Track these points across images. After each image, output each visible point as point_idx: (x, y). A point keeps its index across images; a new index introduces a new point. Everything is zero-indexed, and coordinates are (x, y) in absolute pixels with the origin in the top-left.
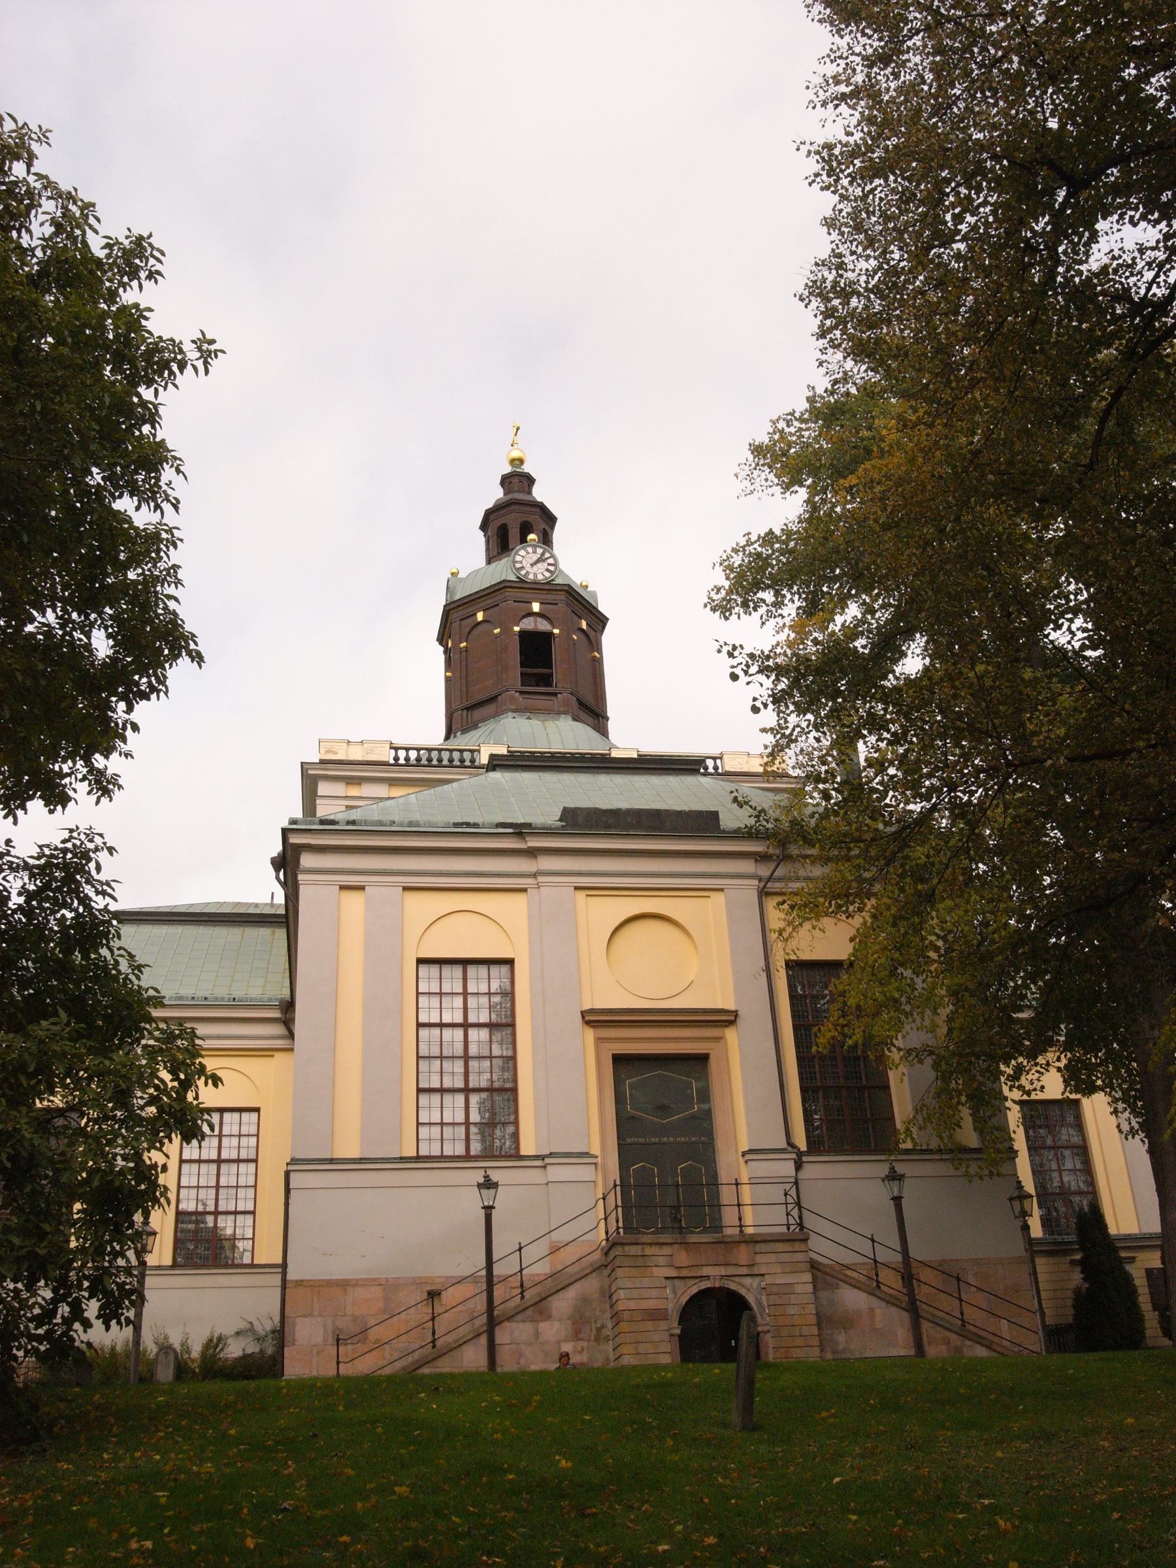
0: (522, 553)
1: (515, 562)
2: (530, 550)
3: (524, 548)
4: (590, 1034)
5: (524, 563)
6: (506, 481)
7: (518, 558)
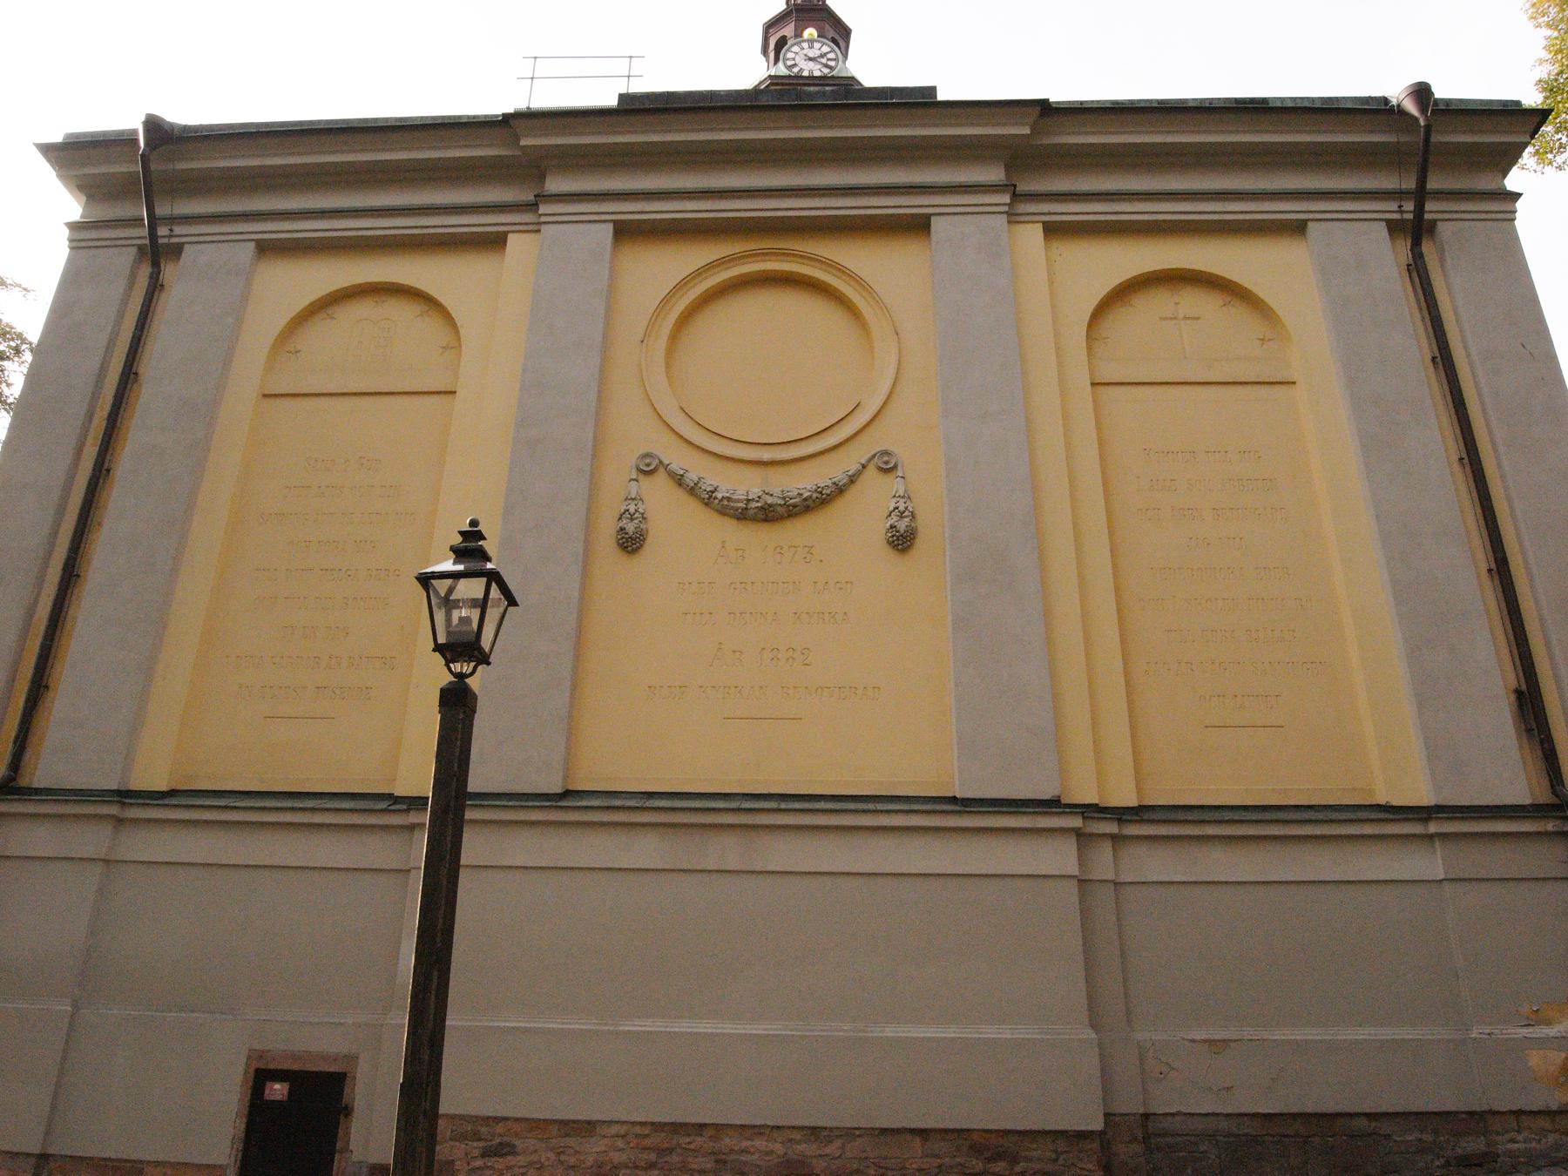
0: (796, 49)
2: (805, 45)
5: (798, 60)
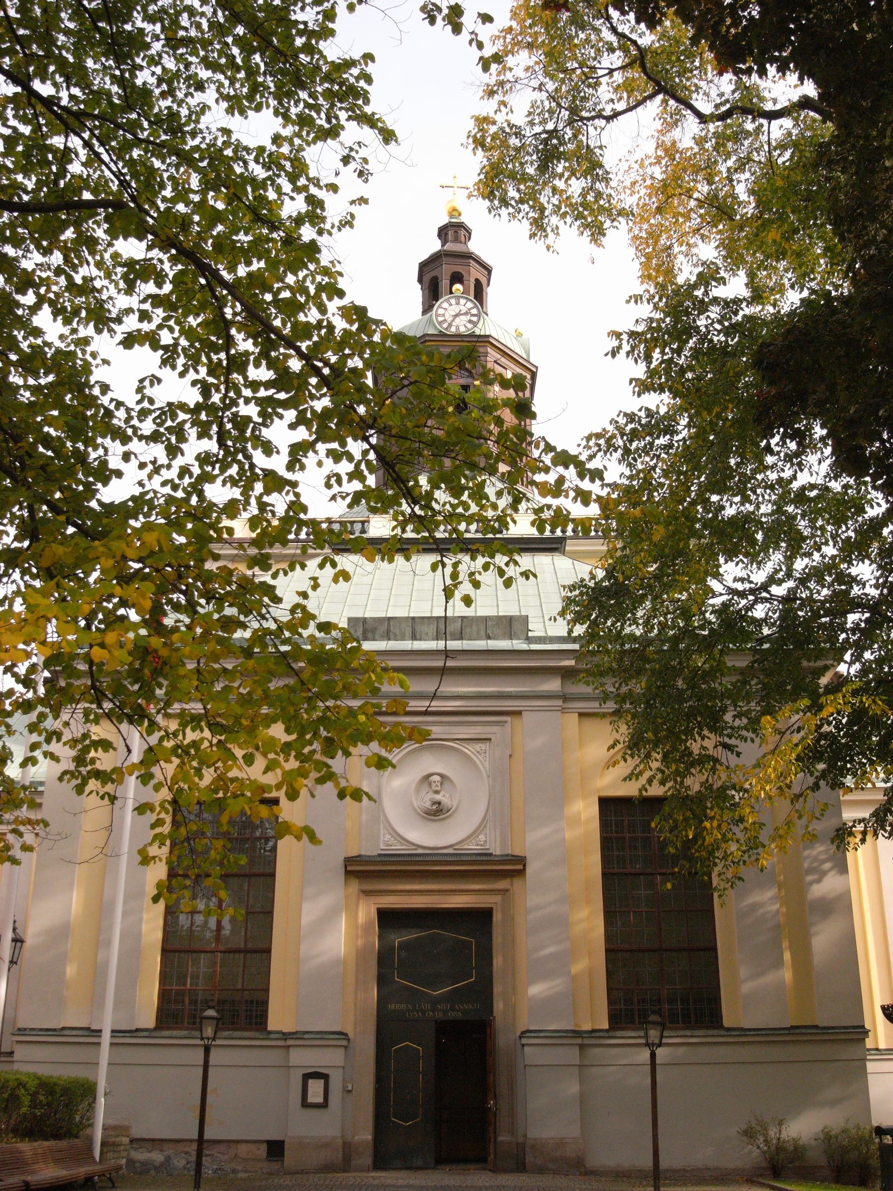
1: (437, 315)
2: (453, 301)
3: (447, 300)
4: (355, 886)
5: (447, 316)
6: (443, 232)
7: (441, 311)
